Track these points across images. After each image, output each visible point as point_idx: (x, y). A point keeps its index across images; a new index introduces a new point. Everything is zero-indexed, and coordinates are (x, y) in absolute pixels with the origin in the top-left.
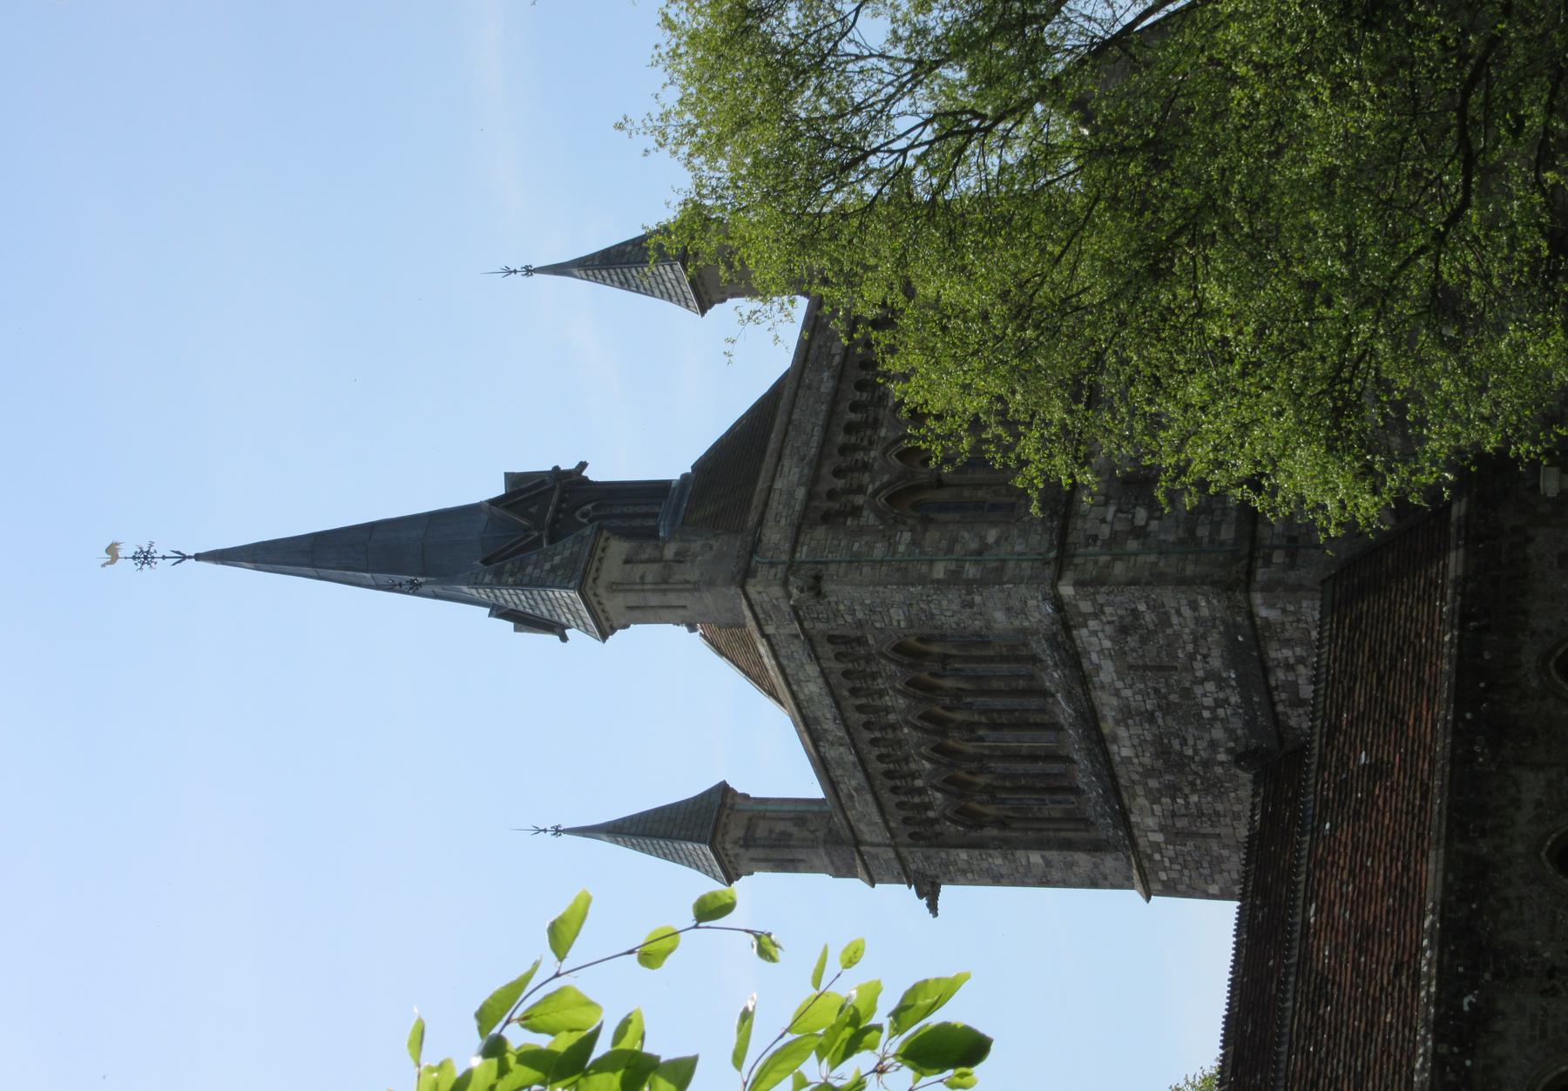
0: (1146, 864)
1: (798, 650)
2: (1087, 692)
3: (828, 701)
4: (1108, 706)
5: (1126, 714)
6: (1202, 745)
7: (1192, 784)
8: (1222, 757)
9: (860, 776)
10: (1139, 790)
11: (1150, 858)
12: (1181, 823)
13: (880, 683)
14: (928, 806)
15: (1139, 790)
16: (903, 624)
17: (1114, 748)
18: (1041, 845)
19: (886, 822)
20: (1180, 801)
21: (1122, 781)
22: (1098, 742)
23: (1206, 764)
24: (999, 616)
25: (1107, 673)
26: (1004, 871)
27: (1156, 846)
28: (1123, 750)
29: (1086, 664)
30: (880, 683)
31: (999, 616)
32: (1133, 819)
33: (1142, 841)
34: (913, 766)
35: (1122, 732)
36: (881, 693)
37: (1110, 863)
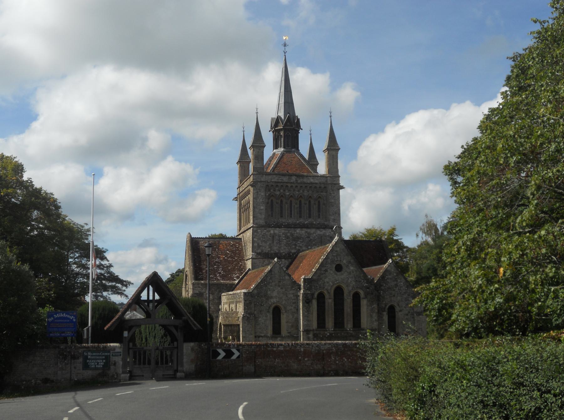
0: (263, 228)
1: (323, 180)
2: (315, 228)
3: (308, 182)
4: (313, 231)
5: (309, 234)
6: (301, 245)
7: (289, 241)
8: (297, 248)
9: (287, 181)
10: (287, 231)
11: (265, 229)
12: (277, 237)
13: (310, 192)
14: (275, 190)
15: (287, 231)
16: (330, 201)
17: (299, 229)
18: (266, 209)
19: (273, 182)
20: (284, 238)
21: (289, 229)
22: (302, 226)
23: (295, 245)
24: (332, 217)
25: (319, 232)
26: (258, 200)
27: (270, 231)
28: (298, 231)
29: (322, 229)
30: (310, 192)
31: (332, 217)
32: (277, 229)
33: (270, 229)
34: (287, 191)
35: (303, 232)
36: (308, 191)
37: (262, 222)
